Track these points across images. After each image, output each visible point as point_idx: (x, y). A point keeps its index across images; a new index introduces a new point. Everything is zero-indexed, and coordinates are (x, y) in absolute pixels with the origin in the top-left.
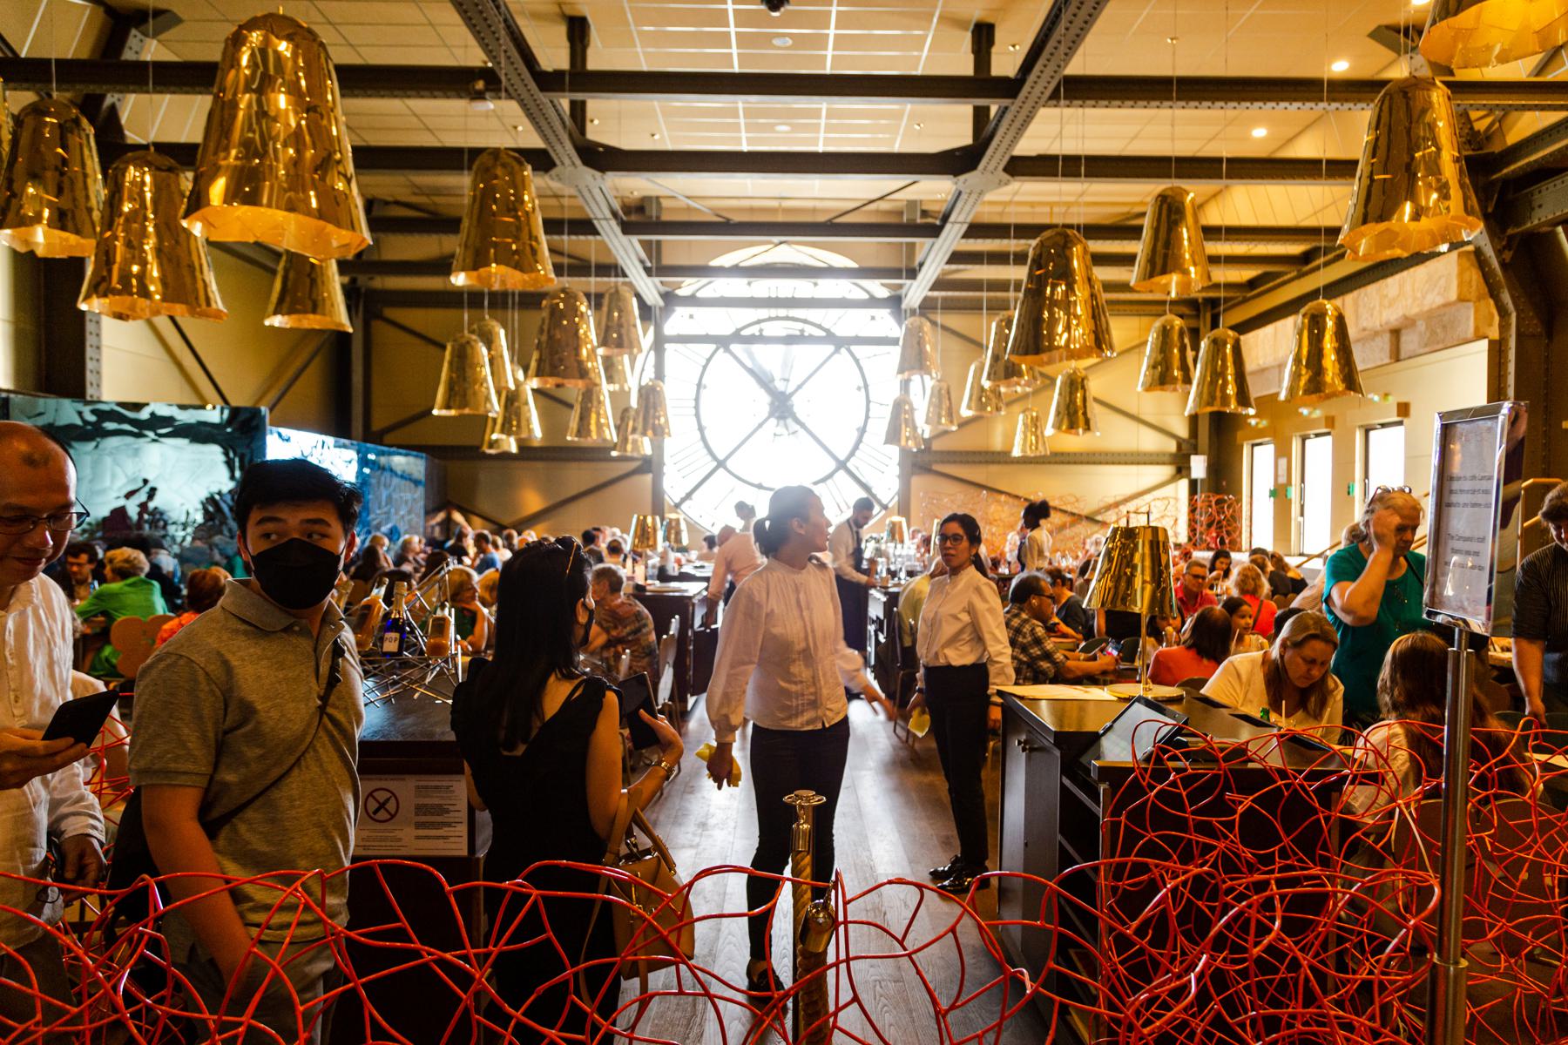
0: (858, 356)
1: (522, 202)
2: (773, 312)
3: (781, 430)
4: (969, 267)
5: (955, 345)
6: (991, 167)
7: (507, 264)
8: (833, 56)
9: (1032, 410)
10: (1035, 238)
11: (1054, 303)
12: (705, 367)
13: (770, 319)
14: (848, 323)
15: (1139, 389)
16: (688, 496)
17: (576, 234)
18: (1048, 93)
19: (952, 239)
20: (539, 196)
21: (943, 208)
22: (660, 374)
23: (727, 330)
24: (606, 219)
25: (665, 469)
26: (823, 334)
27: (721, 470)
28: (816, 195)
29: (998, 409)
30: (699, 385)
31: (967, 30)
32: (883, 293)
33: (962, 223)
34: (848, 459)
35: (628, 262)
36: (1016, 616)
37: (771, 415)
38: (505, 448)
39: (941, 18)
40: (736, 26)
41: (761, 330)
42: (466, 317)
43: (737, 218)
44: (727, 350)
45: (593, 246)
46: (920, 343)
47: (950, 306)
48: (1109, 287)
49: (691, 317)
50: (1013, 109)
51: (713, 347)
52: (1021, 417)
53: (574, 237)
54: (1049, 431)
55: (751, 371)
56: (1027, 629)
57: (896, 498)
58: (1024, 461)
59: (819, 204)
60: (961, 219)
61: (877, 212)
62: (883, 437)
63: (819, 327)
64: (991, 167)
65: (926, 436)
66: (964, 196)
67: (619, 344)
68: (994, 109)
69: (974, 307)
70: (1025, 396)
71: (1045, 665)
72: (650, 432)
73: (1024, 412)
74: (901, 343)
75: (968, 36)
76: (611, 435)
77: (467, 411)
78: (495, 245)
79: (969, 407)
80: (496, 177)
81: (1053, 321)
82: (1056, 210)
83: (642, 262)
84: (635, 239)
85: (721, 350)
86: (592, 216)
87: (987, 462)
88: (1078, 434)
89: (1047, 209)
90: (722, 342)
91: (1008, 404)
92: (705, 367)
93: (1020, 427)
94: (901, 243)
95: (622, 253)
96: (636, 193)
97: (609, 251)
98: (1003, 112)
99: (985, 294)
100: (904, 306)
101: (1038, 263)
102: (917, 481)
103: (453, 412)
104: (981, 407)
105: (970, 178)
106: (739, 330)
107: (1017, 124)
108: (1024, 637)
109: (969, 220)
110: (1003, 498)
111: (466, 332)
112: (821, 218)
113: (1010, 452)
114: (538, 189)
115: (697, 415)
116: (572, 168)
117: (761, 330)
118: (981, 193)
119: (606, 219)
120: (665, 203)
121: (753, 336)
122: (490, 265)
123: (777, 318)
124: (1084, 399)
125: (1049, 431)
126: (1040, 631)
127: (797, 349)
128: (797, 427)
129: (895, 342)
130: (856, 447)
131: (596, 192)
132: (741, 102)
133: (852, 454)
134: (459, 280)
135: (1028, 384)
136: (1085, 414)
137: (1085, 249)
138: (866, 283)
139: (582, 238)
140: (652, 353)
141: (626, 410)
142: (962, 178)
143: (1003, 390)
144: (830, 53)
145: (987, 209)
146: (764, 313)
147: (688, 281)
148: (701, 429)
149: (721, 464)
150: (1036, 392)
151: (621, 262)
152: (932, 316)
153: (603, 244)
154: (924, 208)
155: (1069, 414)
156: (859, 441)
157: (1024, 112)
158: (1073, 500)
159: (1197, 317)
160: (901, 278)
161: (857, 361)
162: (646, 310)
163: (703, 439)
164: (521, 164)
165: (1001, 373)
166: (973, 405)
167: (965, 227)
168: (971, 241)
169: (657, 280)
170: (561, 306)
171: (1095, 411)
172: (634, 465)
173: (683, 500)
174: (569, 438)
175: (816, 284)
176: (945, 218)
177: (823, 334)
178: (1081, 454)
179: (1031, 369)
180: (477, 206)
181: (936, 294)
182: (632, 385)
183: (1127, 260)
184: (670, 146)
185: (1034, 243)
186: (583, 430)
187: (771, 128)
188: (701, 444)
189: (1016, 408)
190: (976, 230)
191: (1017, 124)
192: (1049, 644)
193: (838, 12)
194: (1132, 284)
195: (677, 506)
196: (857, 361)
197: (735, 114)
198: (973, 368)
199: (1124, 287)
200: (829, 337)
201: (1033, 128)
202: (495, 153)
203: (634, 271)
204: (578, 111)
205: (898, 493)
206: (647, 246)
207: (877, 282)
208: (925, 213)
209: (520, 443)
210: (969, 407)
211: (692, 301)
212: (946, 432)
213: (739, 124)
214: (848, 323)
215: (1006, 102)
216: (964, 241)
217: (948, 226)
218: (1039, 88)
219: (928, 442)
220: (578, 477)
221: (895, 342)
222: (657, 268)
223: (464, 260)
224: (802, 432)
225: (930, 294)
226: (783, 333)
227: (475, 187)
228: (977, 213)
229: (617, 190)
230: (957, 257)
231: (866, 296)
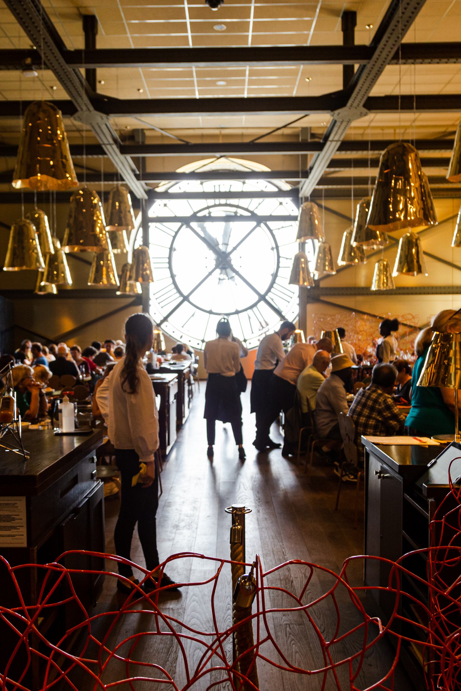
0: (272, 228)
1: (57, 134)
2: (217, 201)
3: (222, 276)
4: (342, 169)
5: (334, 220)
6: (355, 104)
7: (47, 174)
8: (253, 36)
9: (383, 260)
10: (383, 149)
11: (397, 192)
12: (174, 237)
13: (215, 206)
15: (453, 245)
16: (165, 319)
17: (92, 154)
18: (391, 55)
20: (67, 131)
21: (325, 132)
23: (188, 213)
24: (110, 144)
25: (151, 302)
26: (249, 214)
27: (186, 303)
28: (243, 125)
29: (362, 259)
30: (171, 249)
31: (338, 16)
32: (287, 187)
33: (337, 141)
34: (267, 293)
35: (125, 172)
36: (374, 391)
37: (217, 267)
38: (49, 290)
39: (321, 9)
40: (190, 18)
41: (210, 213)
42: (23, 208)
43: (193, 141)
44: (189, 226)
45: (102, 161)
46: (311, 219)
47: (330, 195)
48: (433, 180)
49: (165, 205)
50: (369, 66)
51: (179, 224)
52: (377, 265)
53: (90, 157)
54: (395, 273)
55: (203, 239)
56: (381, 400)
57: (297, 318)
58: (379, 293)
59: (245, 132)
60: (336, 138)
61: (283, 135)
62: (288, 280)
63: (247, 210)
64: (355, 104)
65: (316, 278)
66: (338, 124)
67: (120, 224)
68: (356, 67)
69: (345, 195)
70: (379, 252)
71: (393, 423)
72: (140, 279)
73: (378, 262)
74: (299, 219)
75: (340, 19)
76: (116, 281)
77: (24, 268)
78: (39, 162)
79: (343, 259)
80: (39, 119)
81: (396, 204)
82: (398, 131)
83: (133, 171)
84: (128, 157)
85: (184, 226)
86: (101, 142)
87: (355, 294)
88: (413, 275)
89: (392, 131)
91: (369, 257)
92: (174, 237)
93: (376, 271)
94: (298, 155)
95: (120, 165)
96: (129, 128)
97: (112, 165)
98: (362, 68)
99: (352, 187)
100: (300, 195)
101: (385, 165)
102: (310, 307)
103: (16, 269)
104: (351, 259)
105: (342, 112)
106: (195, 214)
107: (371, 76)
108: (380, 405)
109: (341, 139)
110: (365, 317)
111: (23, 218)
112: (247, 140)
113: (370, 287)
114: (66, 126)
115: (170, 268)
116: (87, 113)
117: (210, 213)
118: (349, 122)
119: (110, 144)
120: (147, 133)
122: (37, 175)
123: (220, 205)
124: (418, 252)
125: (395, 273)
126: (390, 401)
127: (233, 224)
128: (234, 274)
129: (294, 218)
130: (271, 286)
131: (104, 127)
132: (194, 67)
133: (269, 290)
134: (18, 185)
135: (381, 244)
136: (418, 262)
137: (416, 155)
138: (276, 181)
139: (95, 157)
140: (141, 229)
141: (126, 265)
142: (337, 112)
143: (365, 248)
144: (250, 34)
145: (353, 132)
146: (211, 202)
147: (163, 182)
148: (173, 276)
149: (186, 299)
150: (386, 249)
151: (119, 171)
152: (319, 202)
153: (109, 159)
154: (313, 132)
155: (407, 262)
156: (273, 282)
157: (376, 68)
158: (410, 317)
160: (298, 177)
161: (271, 231)
162: (137, 202)
163: (174, 283)
164: (55, 110)
165: (364, 236)
166: (346, 256)
167: (339, 144)
168: (343, 152)
169: (143, 182)
170: (82, 200)
171: (425, 260)
172: (131, 300)
173: (162, 322)
174: (89, 284)
175: (244, 183)
176: (326, 138)
177: (249, 214)
178: (416, 288)
179: (382, 234)
180: (28, 136)
181: (321, 187)
182: (129, 249)
183: (444, 162)
184: (149, 96)
185: (383, 152)
186: (98, 278)
187: (213, 83)
188: (173, 286)
189: (374, 259)
191: (371, 76)
192: (396, 409)
193: (255, 7)
194: (447, 177)
195: (159, 325)
196: (271, 231)
197: (190, 74)
198: (345, 234)
199: (442, 180)
200: (253, 217)
201: (382, 78)
202: (39, 104)
203: (128, 177)
205: (299, 315)
206: (135, 160)
207: (283, 180)
208: (313, 136)
209: (58, 287)
210: (343, 259)
211: (166, 195)
212: (328, 276)
213: (193, 81)
215: (364, 62)
216: (338, 153)
217: (328, 143)
218: (384, 55)
219: (316, 282)
221: (294, 218)
223: (20, 172)
224: (236, 277)
225: (317, 187)
226: (224, 215)
227: (26, 126)
228: (347, 135)
229: (116, 125)
230: (334, 163)
231: (276, 190)
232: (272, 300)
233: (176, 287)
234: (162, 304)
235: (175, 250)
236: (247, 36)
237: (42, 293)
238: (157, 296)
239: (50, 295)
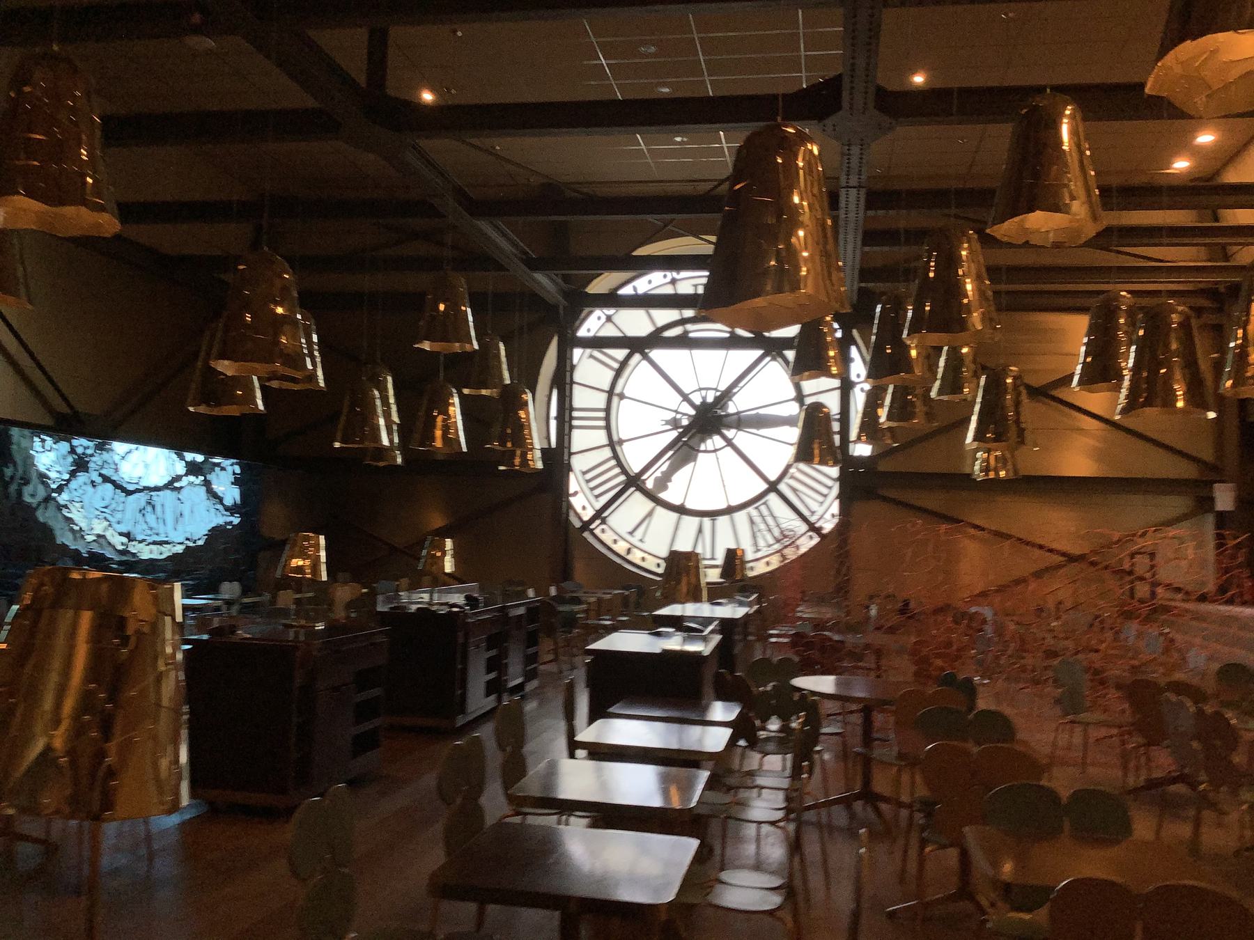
44: (645, 357)
51: (626, 352)
85: (637, 357)
90: (638, 346)
163: (616, 456)
211: (612, 300)
212: (891, 452)
232: (794, 490)
233: (620, 464)
234: (597, 492)
235: (622, 396)
237: (381, 464)
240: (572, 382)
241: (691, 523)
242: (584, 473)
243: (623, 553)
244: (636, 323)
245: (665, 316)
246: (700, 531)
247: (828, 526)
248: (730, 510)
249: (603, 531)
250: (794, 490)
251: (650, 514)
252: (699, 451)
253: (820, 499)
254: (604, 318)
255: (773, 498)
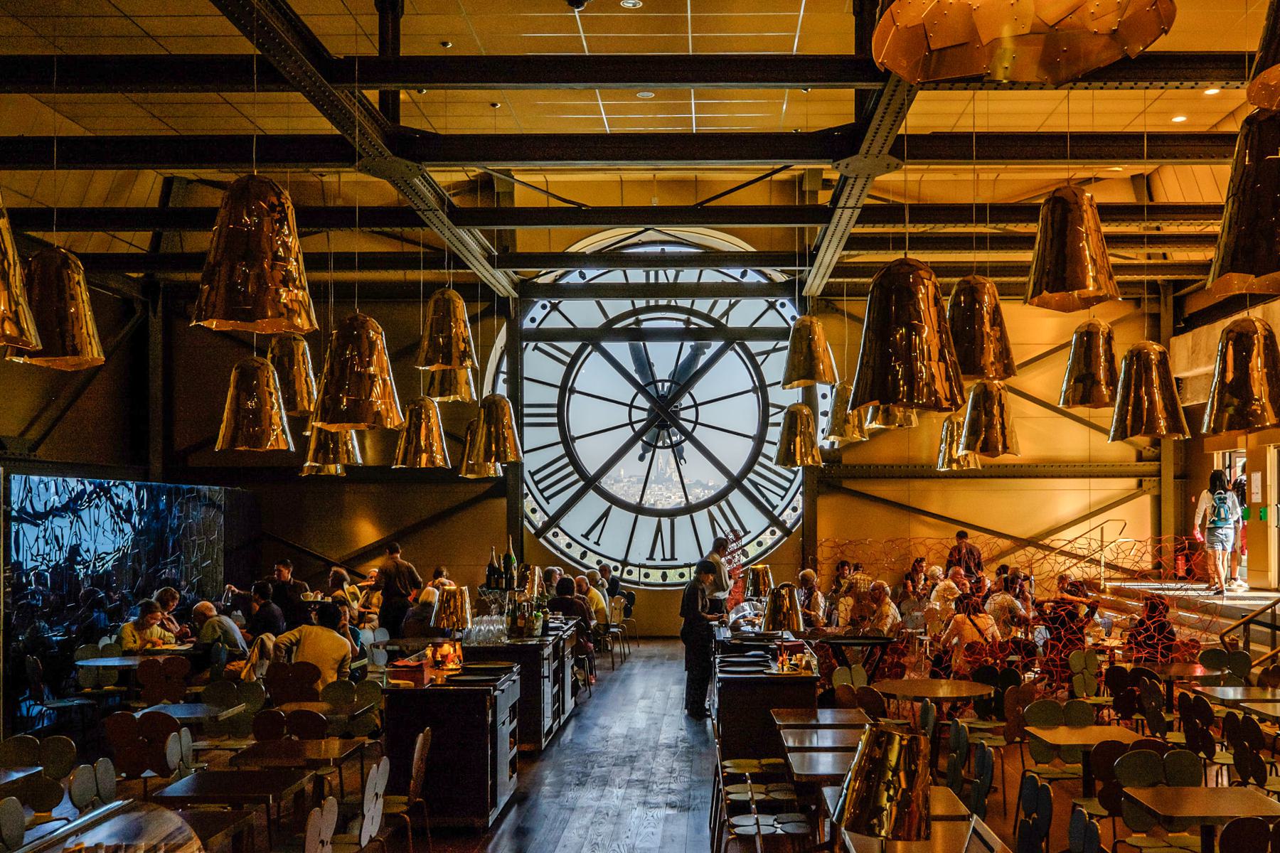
6: (874, 150)
12: (570, 367)
13: (648, 309)
14: (745, 313)
16: (553, 521)
19: (845, 222)
22: (516, 380)
23: (597, 321)
27: (591, 494)
43: (591, 201)
49: (555, 307)
51: (579, 344)
60: (851, 203)
64: (874, 150)
66: (851, 181)
85: (590, 348)
90: (591, 339)
92: (570, 367)
105: (854, 163)
107: (895, 106)
109: (860, 205)
121: (625, 329)
142: (843, 162)
146: (640, 303)
149: (591, 483)
159: (1158, 301)
161: (752, 357)
167: (857, 212)
169: (510, 271)
190: (868, 214)
196: (752, 357)
204: (390, 104)
205: (802, 515)
211: (557, 291)
214: (745, 313)
217: (839, 212)
220: (426, 502)
222: (505, 257)
230: (854, 242)
236: (687, 17)
238: (537, 478)
239: (335, 478)
240: (522, 378)
241: (647, 525)
242: (532, 474)
243: (578, 557)
244: (585, 313)
245: (616, 307)
246: (659, 529)
247: (789, 517)
248: (689, 509)
249: (556, 535)
250: (755, 485)
251: (606, 514)
252: (656, 447)
253: (782, 493)
254: (549, 305)
255: (736, 497)
